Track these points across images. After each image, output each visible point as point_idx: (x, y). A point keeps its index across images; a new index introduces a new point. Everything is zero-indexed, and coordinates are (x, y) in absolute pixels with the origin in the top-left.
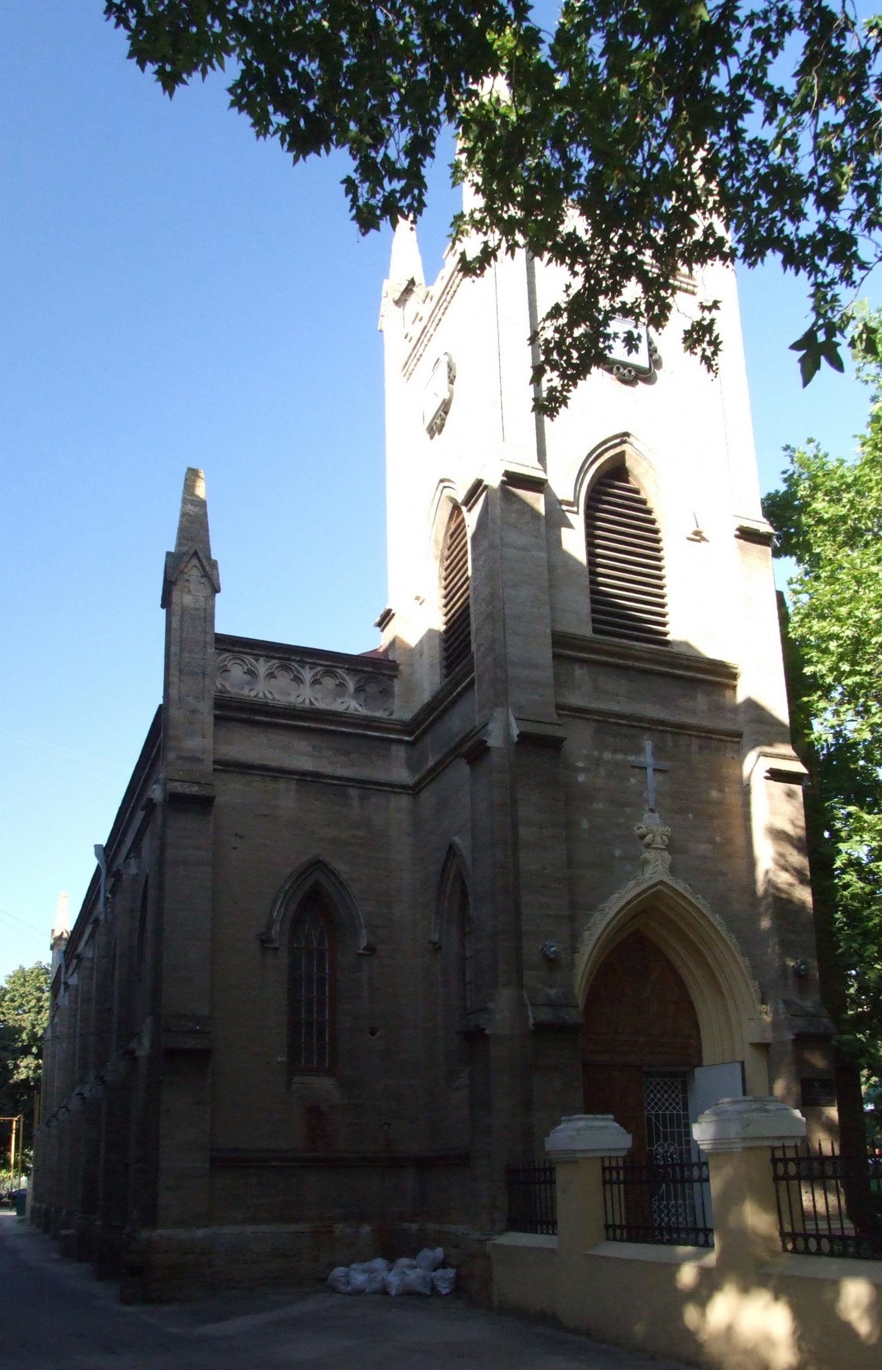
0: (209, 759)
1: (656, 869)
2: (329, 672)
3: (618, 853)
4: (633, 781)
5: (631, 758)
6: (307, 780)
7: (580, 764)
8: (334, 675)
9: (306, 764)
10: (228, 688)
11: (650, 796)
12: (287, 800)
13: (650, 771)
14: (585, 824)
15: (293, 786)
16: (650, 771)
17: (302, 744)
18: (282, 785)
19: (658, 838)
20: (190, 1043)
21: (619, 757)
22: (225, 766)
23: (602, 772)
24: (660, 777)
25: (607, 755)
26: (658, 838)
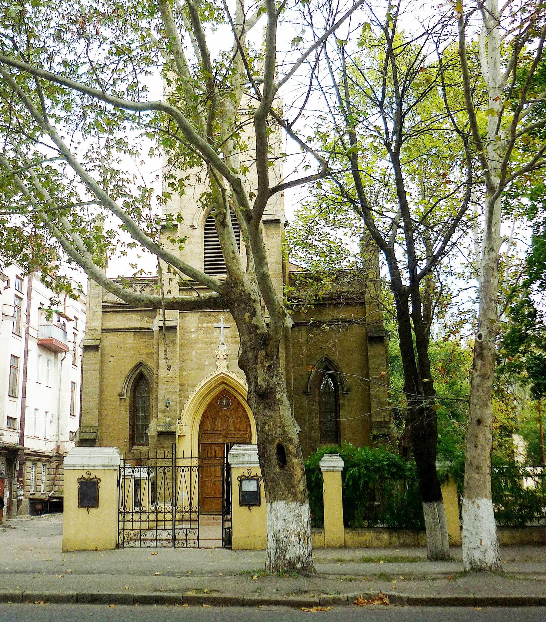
0: (100, 329)
1: (222, 368)
2: (147, 285)
3: (207, 363)
4: (215, 333)
5: (215, 325)
6: (137, 331)
7: (193, 330)
8: (149, 286)
9: (138, 325)
10: (109, 299)
11: (222, 338)
12: (130, 339)
13: (222, 328)
14: (194, 353)
15: (132, 334)
16: (222, 328)
17: (136, 317)
18: (128, 334)
19: (222, 356)
20: (88, 437)
21: (210, 325)
22: (106, 330)
23: (202, 332)
24: (227, 329)
25: (205, 325)
26: (222, 356)
